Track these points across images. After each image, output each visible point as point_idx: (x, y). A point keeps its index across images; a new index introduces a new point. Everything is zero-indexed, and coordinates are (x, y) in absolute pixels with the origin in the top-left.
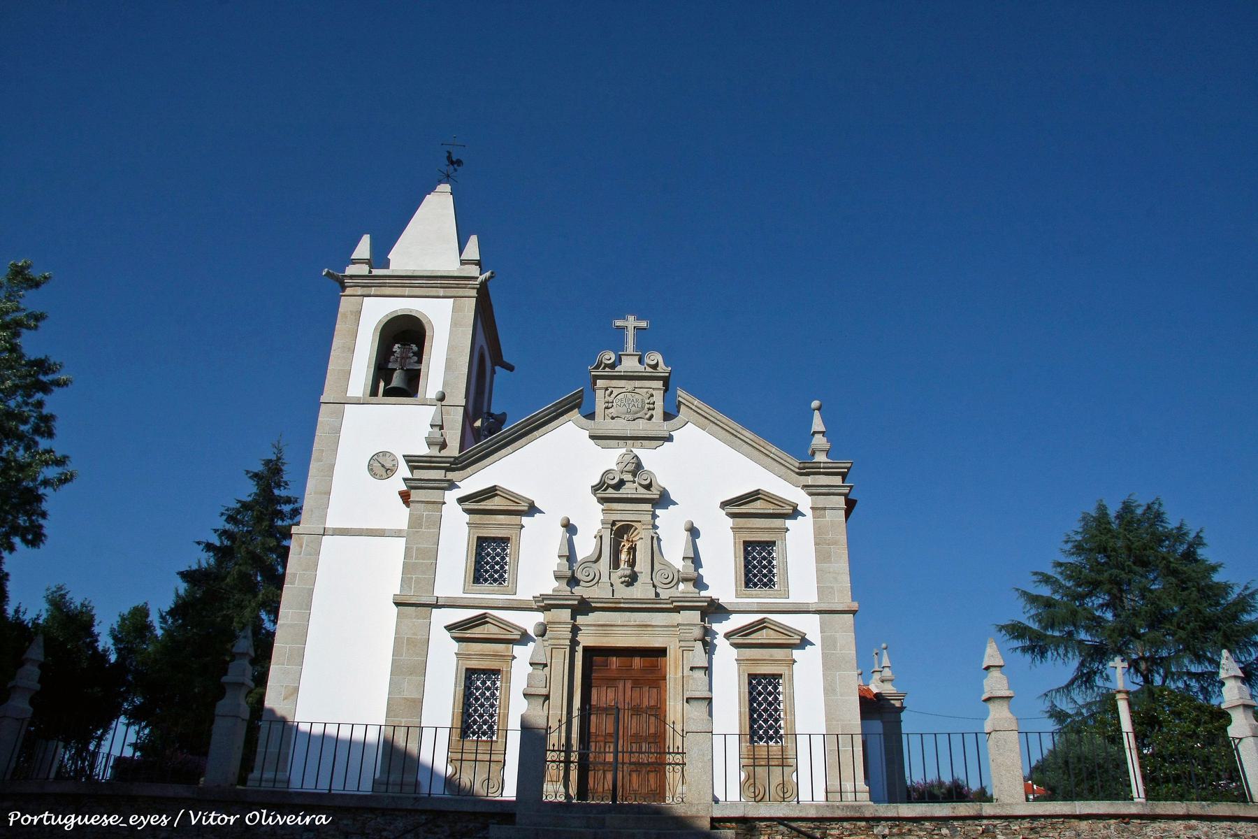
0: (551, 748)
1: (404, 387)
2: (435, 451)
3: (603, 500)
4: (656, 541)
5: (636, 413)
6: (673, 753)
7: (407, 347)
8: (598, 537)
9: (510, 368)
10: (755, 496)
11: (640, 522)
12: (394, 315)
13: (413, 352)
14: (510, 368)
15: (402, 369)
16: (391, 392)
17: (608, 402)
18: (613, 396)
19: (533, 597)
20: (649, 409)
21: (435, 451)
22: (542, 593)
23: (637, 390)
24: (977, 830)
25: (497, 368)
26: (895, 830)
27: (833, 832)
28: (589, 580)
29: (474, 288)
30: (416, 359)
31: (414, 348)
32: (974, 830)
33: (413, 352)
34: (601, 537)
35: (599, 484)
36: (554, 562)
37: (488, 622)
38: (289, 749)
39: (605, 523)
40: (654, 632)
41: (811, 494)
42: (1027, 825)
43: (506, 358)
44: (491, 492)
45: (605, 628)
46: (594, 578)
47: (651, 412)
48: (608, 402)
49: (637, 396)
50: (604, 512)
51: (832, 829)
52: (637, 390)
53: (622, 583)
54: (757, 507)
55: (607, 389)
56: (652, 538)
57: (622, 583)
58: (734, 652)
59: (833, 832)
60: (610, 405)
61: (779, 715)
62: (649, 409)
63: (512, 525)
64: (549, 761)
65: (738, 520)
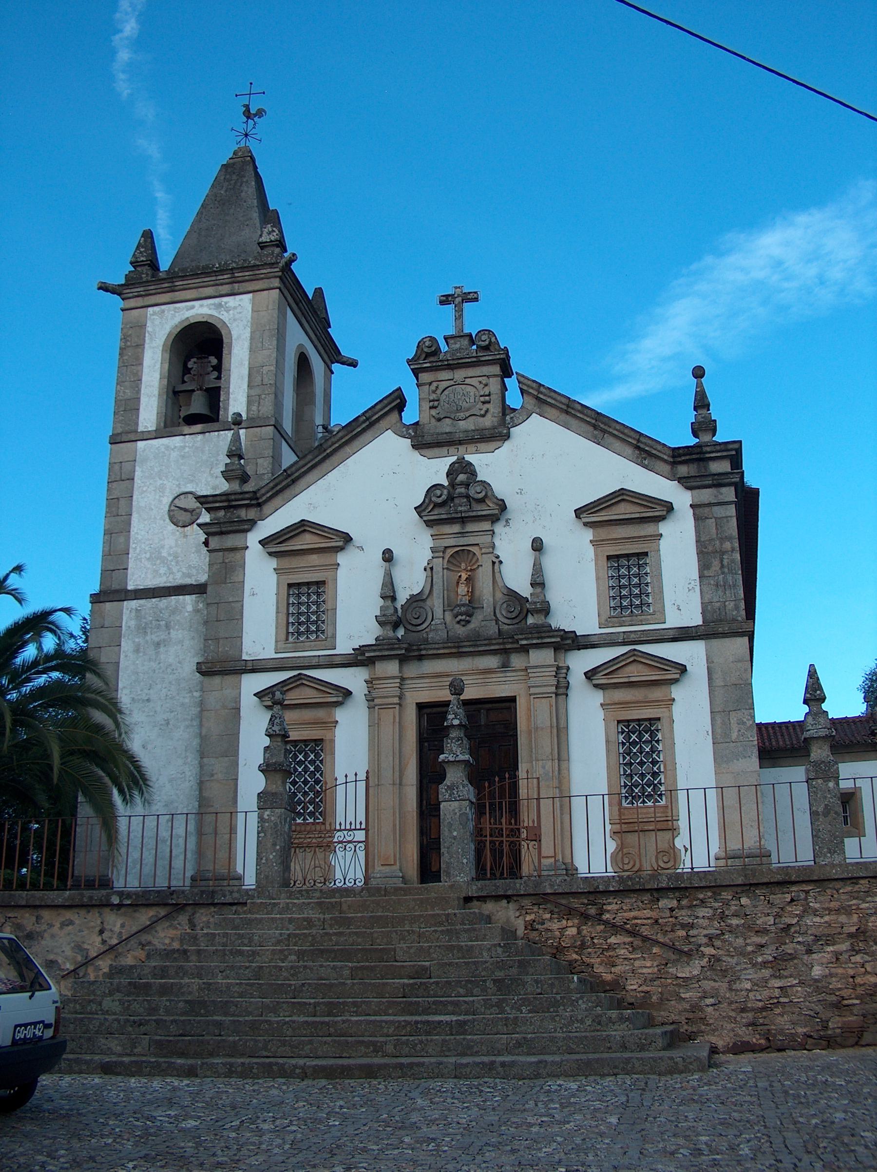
0: (338, 827)
1: (209, 414)
2: (236, 486)
3: (429, 524)
4: (497, 562)
5: (468, 410)
6: (345, 830)
7: (203, 360)
8: (428, 569)
9: (353, 364)
10: (621, 496)
11: (478, 544)
12: (186, 324)
13: (212, 366)
14: (353, 364)
15: (201, 389)
16: (192, 420)
17: (433, 401)
18: (439, 392)
19: (353, 649)
20: (484, 403)
21: (236, 486)
22: (361, 644)
23: (468, 381)
24: (785, 898)
25: (335, 367)
26: (684, 902)
27: (609, 907)
28: (414, 623)
29: (276, 277)
30: (215, 374)
31: (214, 361)
32: (780, 898)
33: (212, 366)
34: (432, 569)
35: (421, 505)
36: (374, 605)
37: (303, 684)
38: (70, 846)
39: (436, 552)
40: (414, 686)
41: (688, 488)
42: (849, 889)
43: (345, 352)
44: (302, 527)
45: (440, 679)
46: (425, 620)
47: (487, 406)
48: (433, 401)
49: (469, 388)
50: (434, 538)
51: (609, 904)
52: (468, 381)
53: (458, 622)
54: (306, 541)
55: (430, 384)
56: (494, 563)
57: (458, 622)
58: (598, 697)
59: (609, 907)
60: (436, 403)
61: (659, 768)
62: (484, 403)
63: (326, 565)
64: (336, 842)
65: (600, 530)
